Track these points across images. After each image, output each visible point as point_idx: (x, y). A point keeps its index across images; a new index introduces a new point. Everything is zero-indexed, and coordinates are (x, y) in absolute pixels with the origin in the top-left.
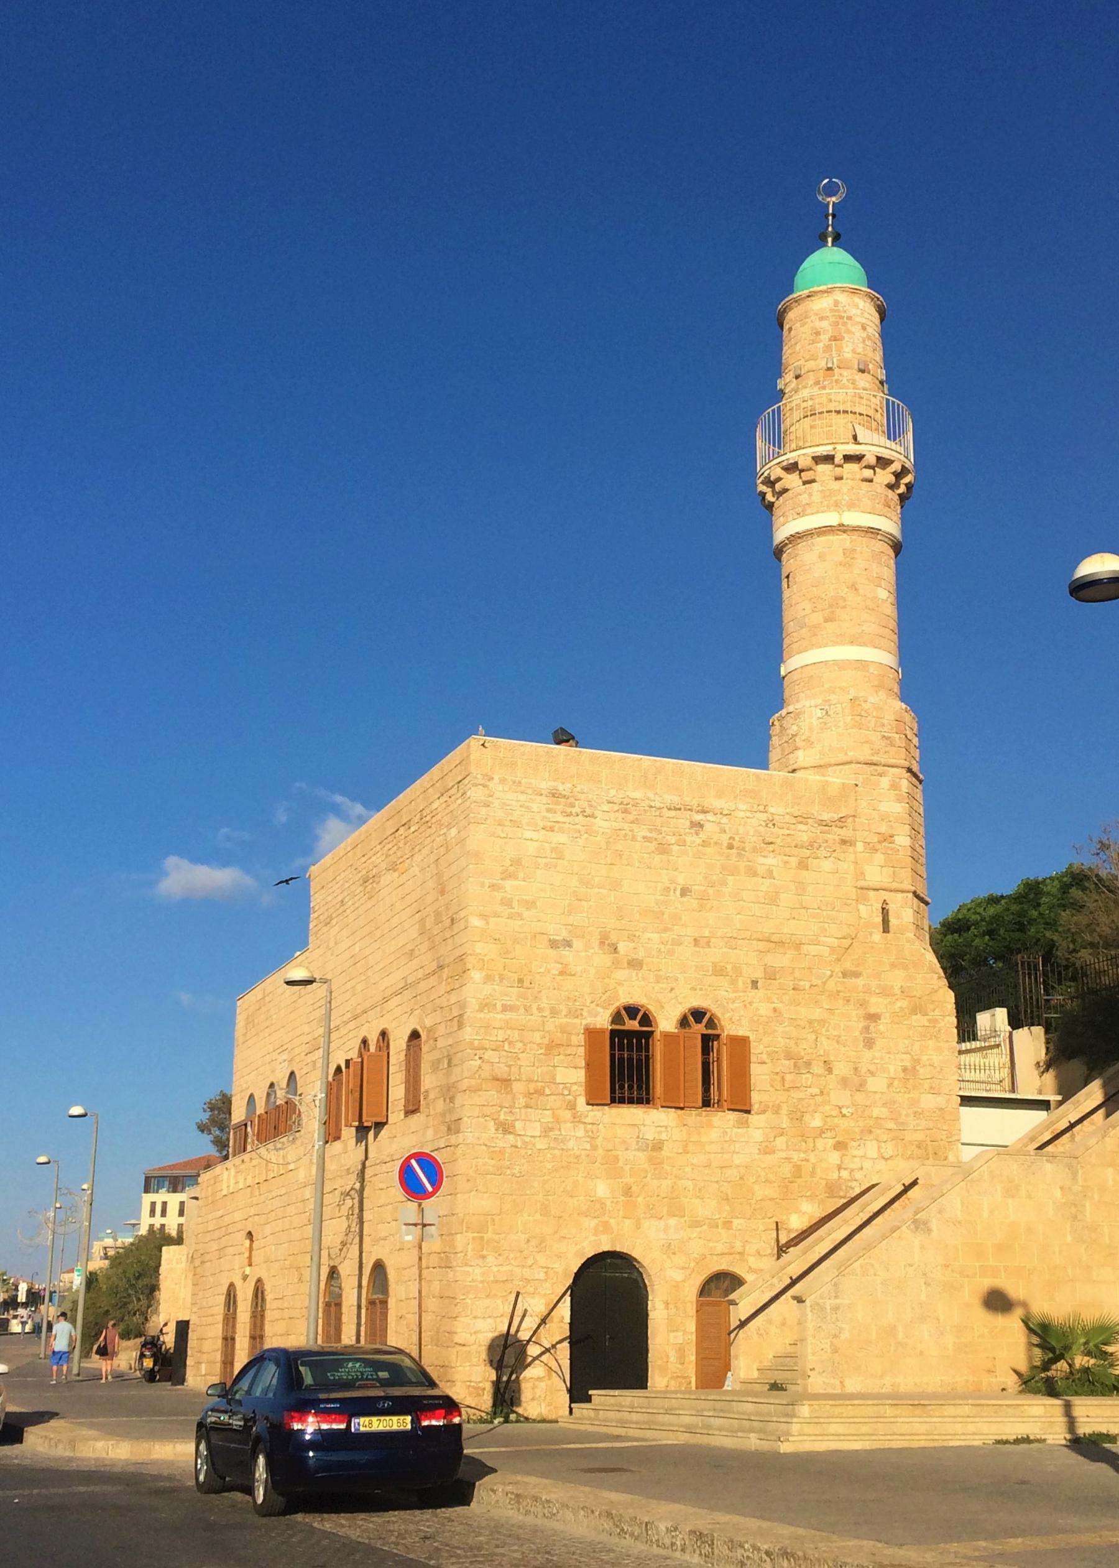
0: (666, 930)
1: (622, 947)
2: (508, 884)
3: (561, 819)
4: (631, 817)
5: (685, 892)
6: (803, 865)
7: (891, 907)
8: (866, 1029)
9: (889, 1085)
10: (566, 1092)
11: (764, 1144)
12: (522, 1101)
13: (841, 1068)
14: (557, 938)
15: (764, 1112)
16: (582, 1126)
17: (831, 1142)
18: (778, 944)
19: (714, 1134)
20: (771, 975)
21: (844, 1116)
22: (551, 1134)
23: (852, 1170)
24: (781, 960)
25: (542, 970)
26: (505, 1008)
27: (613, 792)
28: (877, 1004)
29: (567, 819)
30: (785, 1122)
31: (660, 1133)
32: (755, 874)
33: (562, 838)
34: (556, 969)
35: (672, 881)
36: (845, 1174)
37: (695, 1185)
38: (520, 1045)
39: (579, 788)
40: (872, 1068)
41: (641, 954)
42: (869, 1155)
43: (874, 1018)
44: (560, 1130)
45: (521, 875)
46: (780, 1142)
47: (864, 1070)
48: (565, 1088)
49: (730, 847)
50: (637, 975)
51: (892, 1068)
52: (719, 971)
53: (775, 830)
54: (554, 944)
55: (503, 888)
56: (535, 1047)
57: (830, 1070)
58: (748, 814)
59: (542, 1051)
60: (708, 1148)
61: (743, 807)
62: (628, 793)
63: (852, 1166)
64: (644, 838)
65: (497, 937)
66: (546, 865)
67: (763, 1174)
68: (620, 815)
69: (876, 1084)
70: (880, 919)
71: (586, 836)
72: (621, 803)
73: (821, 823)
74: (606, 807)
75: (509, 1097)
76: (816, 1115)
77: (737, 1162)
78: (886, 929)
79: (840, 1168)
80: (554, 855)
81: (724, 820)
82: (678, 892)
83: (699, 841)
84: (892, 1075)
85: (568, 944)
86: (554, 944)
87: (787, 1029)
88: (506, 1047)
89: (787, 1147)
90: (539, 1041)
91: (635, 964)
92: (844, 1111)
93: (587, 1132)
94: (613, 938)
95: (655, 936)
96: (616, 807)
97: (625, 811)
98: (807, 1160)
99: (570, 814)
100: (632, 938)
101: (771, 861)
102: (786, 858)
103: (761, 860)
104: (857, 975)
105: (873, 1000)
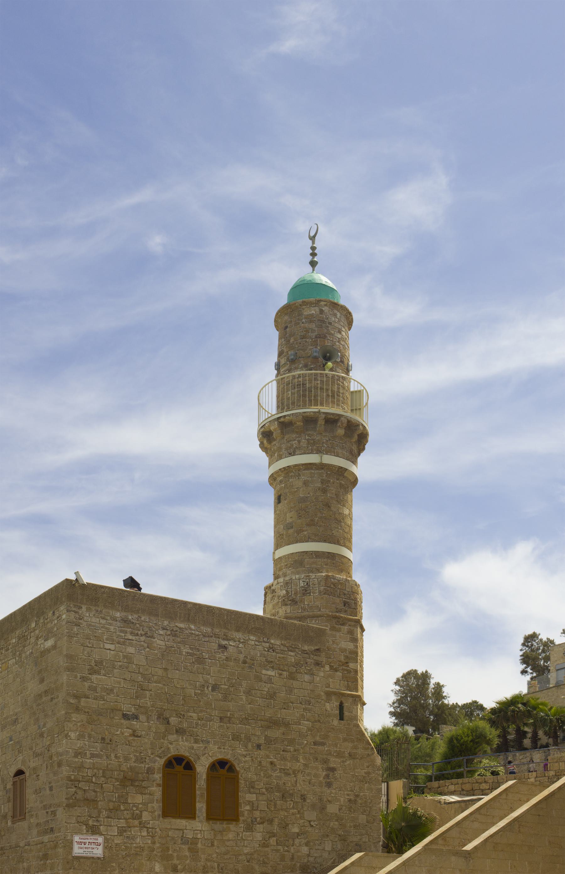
0: (201, 711)
1: (173, 720)
2: (94, 677)
3: (130, 637)
4: (179, 640)
5: (215, 688)
6: (292, 677)
7: (346, 705)
8: (327, 776)
9: (340, 810)
10: (134, 809)
11: (263, 842)
12: (104, 813)
13: (311, 798)
14: (128, 713)
15: (262, 823)
16: (145, 829)
17: (304, 841)
18: (274, 723)
19: (231, 836)
20: (269, 741)
21: (312, 826)
22: (125, 834)
23: (316, 857)
24: (275, 733)
25: (118, 733)
26: (93, 756)
27: (166, 623)
28: (334, 762)
29: (134, 638)
30: (275, 828)
31: (197, 834)
32: (261, 680)
33: (131, 650)
34: (127, 732)
35: (207, 682)
36: (311, 859)
37: (218, 865)
38: (103, 779)
39: (143, 618)
40: (330, 799)
41: (185, 725)
42: (326, 849)
43: (333, 770)
44: (130, 831)
45: (103, 672)
46: (273, 841)
47: (325, 800)
48: (134, 806)
49: (245, 662)
50: (182, 738)
51: (342, 799)
52: (236, 738)
53: (274, 654)
54: (125, 716)
55: (90, 679)
56: (114, 780)
57: (304, 800)
58: (256, 643)
59: (118, 783)
60: (228, 843)
61: (252, 638)
62: (177, 624)
63: (316, 855)
64: (188, 653)
65: (86, 710)
66: (120, 666)
67: (261, 859)
68: (171, 638)
69: (332, 809)
70: (338, 712)
71: (148, 649)
72: (172, 630)
73: (304, 652)
74: (161, 632)
75: (96, 811)
76: (295, 825)
77: (246, 852)
78: (341, 718)
79: (308, 855)
80: (125, 660)
81: (241, 645)
82: (210, 688)
83: (224, 657)
84: (342, 803)
85: (136, 717)
86: (125, 716)
87: (279, 774)
88: (94, 780)
89: (277, 843)
90: (116, 776)
91: (180, 731)
92: (312, 823)
93: (148, 833)
94: (167, 714)
95: (194, 715)
96: (169, 633)
97: (175, 636)
98: (288, 851)
99: (137, 635)
100: (178, 715)
101: (271, 673)
102: (280, 671)
103: (264, 672)
104: (323, 744)
105: (332, 759)
